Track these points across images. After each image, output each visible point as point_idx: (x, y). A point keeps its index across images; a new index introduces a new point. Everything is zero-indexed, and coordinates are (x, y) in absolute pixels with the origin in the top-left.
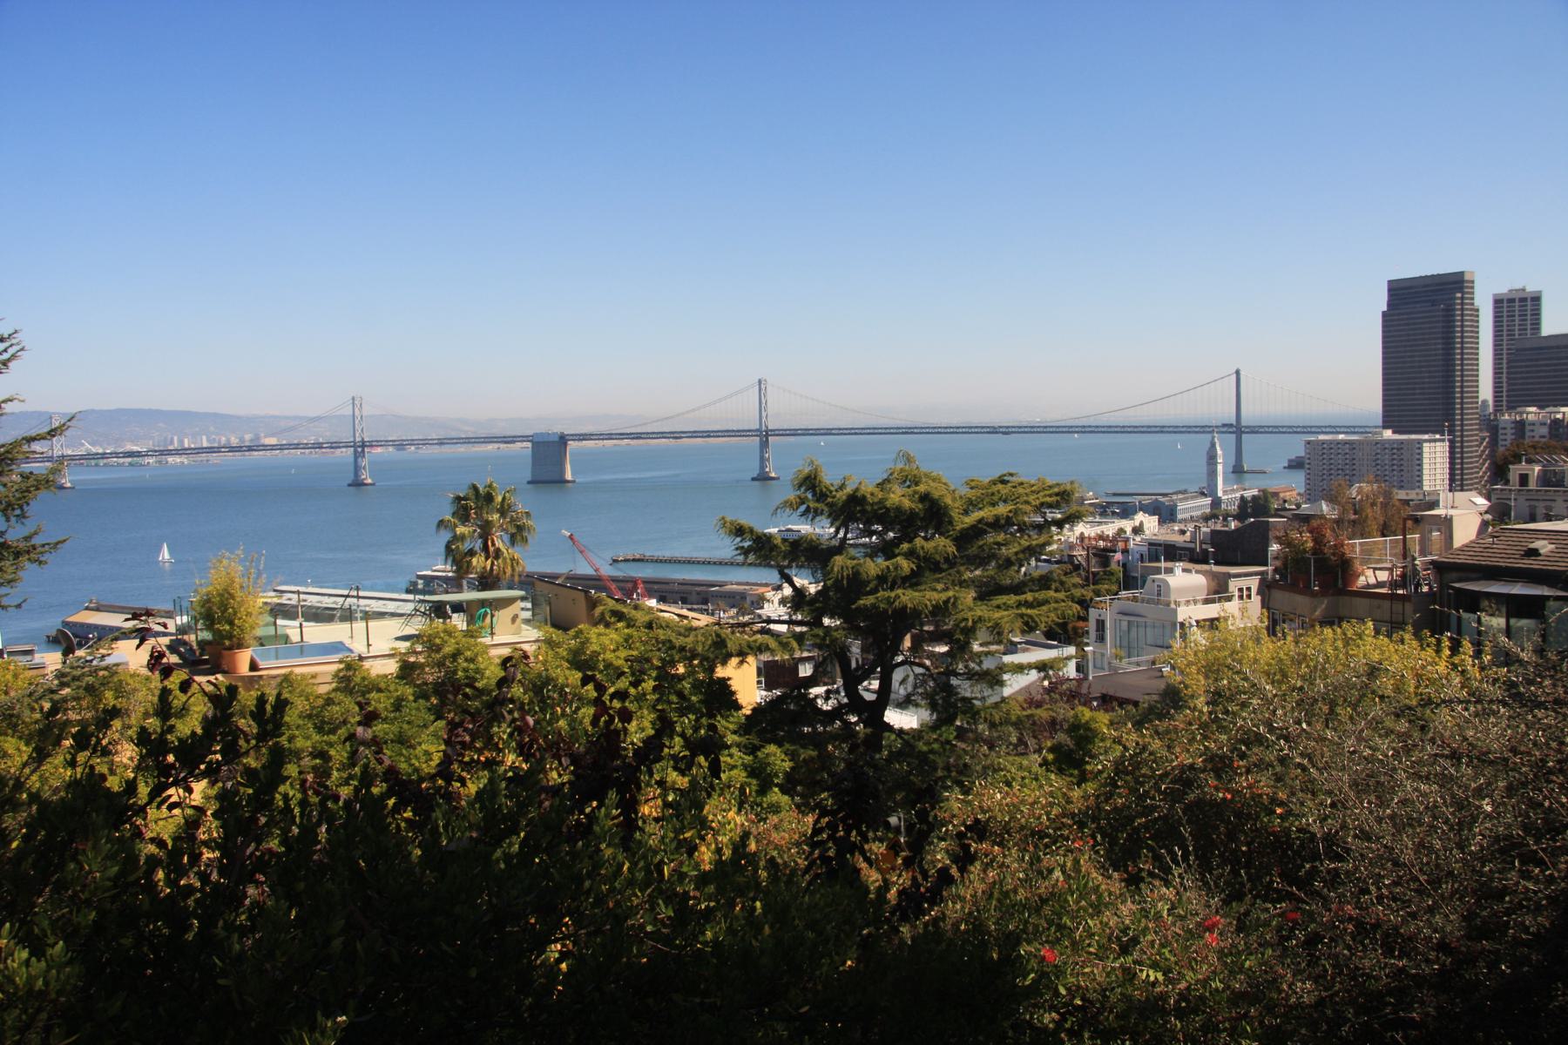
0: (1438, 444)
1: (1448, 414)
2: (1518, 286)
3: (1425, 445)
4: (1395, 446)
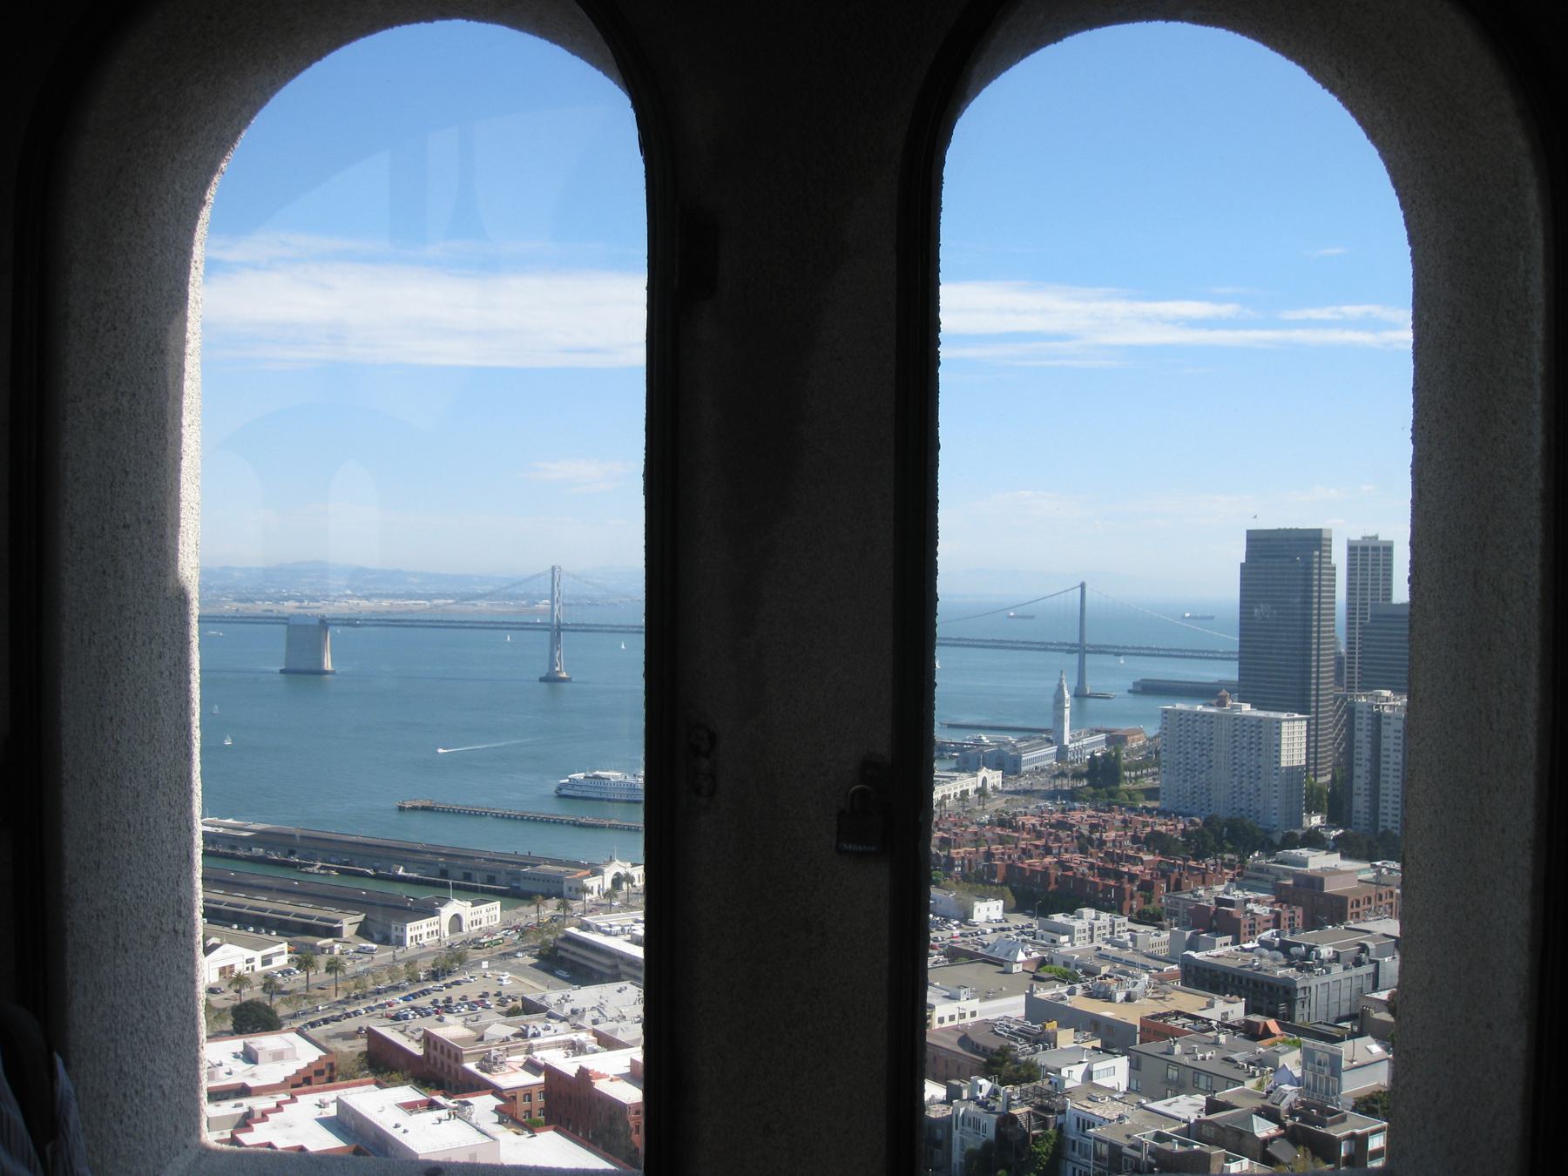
0: (1296, 723)
1: (1305, 693)
2: (1371, 533)
3: (1284, 724)
4: (1254, 723)
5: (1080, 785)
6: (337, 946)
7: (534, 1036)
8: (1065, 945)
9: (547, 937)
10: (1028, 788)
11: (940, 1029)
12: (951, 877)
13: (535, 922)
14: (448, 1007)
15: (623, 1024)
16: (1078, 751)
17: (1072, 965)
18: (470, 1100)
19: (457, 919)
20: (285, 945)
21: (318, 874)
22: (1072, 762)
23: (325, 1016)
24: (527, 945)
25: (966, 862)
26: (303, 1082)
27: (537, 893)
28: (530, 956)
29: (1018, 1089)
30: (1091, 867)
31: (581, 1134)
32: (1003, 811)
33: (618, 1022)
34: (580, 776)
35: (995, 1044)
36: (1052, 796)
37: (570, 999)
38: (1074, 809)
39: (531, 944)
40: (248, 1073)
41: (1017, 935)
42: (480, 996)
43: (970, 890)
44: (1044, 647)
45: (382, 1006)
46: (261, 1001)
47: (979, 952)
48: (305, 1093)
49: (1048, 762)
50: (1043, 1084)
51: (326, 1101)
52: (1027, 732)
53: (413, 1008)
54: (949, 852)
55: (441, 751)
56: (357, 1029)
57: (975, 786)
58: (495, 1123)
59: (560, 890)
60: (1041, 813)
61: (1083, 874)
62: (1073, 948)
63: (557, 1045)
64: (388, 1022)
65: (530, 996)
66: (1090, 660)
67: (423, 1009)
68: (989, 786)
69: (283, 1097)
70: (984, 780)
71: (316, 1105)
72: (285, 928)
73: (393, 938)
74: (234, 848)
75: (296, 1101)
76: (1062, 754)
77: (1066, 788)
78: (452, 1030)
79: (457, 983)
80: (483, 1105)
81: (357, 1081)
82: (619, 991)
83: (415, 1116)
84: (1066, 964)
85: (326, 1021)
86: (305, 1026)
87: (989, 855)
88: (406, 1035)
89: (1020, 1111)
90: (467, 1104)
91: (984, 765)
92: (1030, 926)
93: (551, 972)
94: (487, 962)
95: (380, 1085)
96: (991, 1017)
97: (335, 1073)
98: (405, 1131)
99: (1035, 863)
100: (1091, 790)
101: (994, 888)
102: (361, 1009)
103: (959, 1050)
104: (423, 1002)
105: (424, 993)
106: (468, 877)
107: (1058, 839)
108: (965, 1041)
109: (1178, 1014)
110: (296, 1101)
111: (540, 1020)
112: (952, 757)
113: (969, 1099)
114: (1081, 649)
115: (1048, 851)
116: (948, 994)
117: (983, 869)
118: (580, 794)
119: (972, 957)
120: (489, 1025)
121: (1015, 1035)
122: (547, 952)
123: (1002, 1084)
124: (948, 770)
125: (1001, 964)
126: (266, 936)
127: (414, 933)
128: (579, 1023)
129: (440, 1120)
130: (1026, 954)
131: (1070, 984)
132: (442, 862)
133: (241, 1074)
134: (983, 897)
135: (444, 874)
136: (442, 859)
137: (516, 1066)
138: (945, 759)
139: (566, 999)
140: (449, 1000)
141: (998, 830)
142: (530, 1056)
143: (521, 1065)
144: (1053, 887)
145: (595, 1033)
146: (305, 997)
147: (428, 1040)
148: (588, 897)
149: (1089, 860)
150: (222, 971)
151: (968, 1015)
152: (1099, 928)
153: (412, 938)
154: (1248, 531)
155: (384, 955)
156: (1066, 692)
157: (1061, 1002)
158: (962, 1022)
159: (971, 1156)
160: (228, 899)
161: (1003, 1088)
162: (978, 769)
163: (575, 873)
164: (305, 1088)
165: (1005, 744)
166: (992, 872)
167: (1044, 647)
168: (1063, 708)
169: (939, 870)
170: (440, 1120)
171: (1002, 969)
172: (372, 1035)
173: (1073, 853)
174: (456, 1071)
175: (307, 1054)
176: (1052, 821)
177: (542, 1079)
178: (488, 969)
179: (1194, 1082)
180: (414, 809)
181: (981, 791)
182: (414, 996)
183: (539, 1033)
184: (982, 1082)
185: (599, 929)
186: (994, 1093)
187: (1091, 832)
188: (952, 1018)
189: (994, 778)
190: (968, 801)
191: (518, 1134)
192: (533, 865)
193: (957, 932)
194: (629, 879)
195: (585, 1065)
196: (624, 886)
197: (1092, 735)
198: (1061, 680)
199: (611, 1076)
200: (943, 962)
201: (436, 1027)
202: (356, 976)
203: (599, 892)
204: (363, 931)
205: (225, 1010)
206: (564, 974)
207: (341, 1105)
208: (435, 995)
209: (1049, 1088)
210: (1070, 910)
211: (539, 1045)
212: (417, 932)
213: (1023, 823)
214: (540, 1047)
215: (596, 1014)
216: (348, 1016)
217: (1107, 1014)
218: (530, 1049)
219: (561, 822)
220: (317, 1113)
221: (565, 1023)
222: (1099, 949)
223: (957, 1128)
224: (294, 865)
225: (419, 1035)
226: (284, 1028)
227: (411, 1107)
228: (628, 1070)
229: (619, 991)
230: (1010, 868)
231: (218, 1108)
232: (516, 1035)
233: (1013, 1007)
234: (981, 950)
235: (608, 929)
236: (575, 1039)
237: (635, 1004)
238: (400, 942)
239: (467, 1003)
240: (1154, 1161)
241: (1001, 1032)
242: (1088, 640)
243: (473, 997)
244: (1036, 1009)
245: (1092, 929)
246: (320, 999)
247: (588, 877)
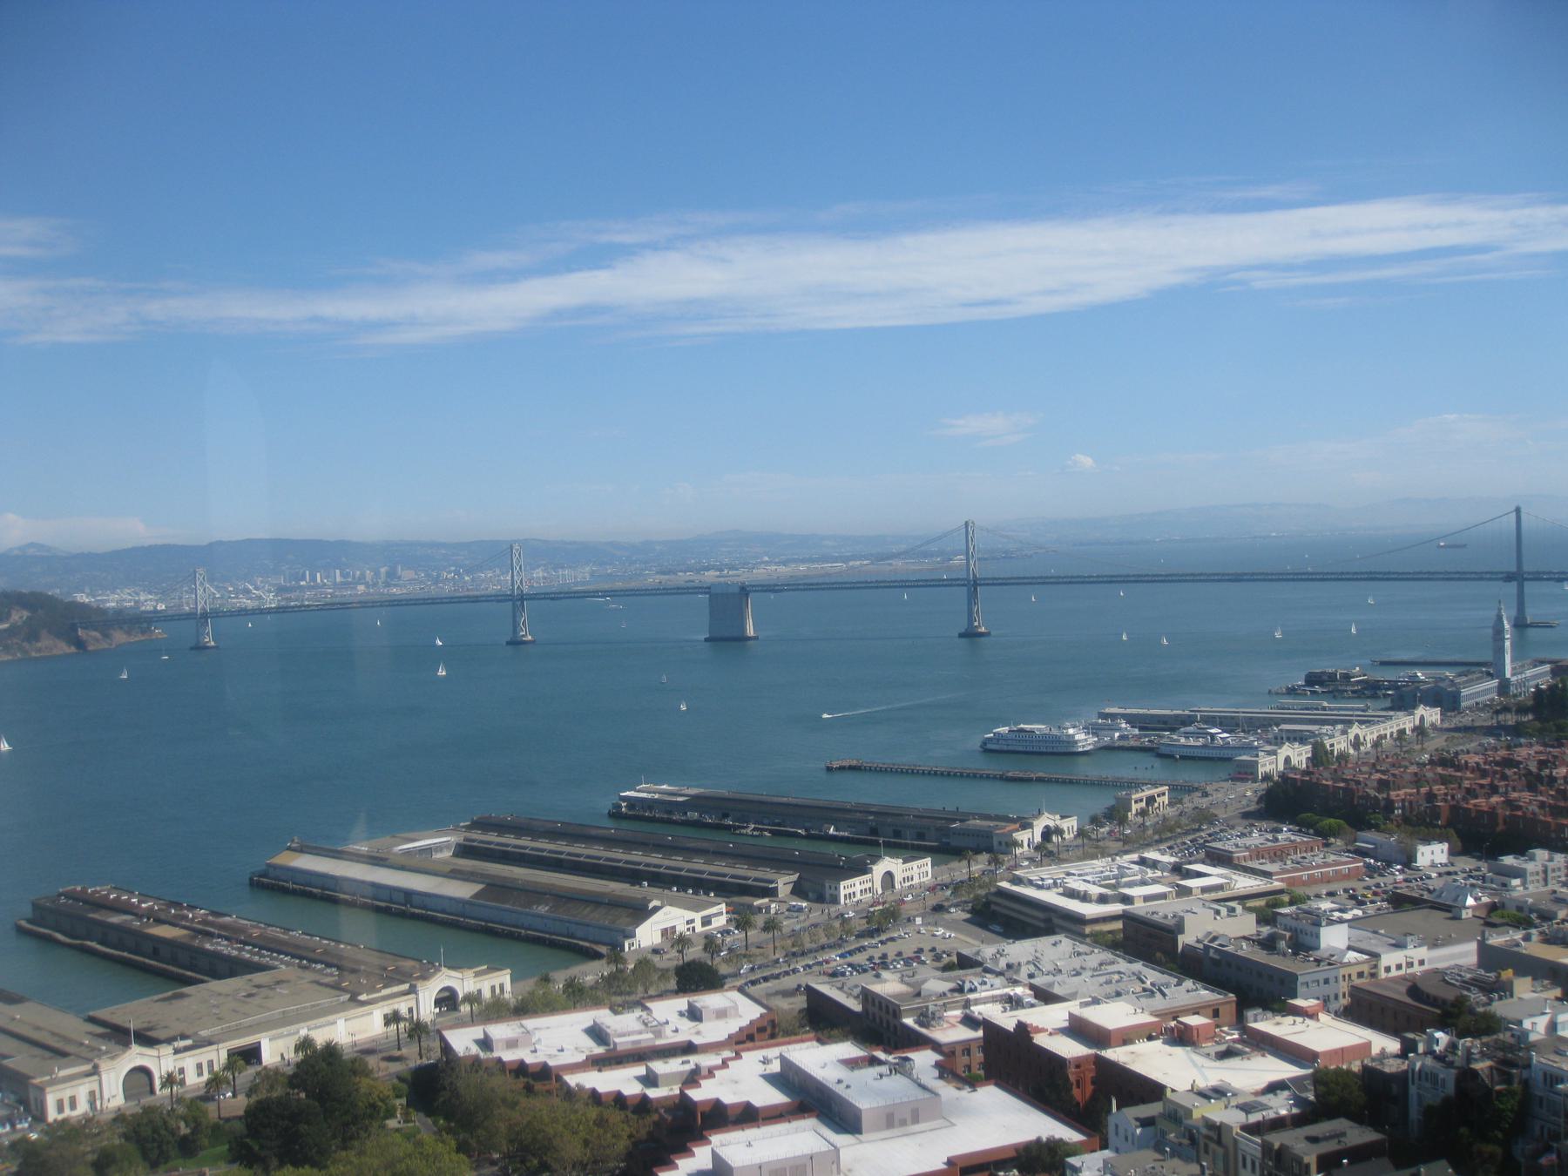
5: (1525, 719)
6: (773, 905)
7: (972, 990)
8: (1518, 888)
9: (979, 892)
10: (1470, 724)
11: (1387, 979)
12: (1391, 820)
13: (967, 877)
14: (884, 963)
15: (1059, 978)
16: (1522, 683)
17: (1526, 909)
18: (910, 1055)
19: (889, 876)
20: (724, 905)
21: (752, 836)
22: (1515, 696)
23: (765, 974)
24: (959, 900)
25: (1407, 804)
26: (747, 1039)
27: (967, 849)
28: (963, 910)
29: (1477, 1042)
30: (1542, 805)
31: (1021, 1088)
32: (1443, 750)
33: (1054, 976)
34: (1004, 730)
35: (1450, 995)
36: (1489, 731)
37: (1005, 953)
38: (1521, 745)
39: (963, 899)
40: (694, 1031)
41: (1464, 879)
42: (915, 952)
43: (1412, 834)
44: (1480, 577)
45: (820, 964)
46: (702, 960)
47: (1425, 897)
48: (749, 1049)
49: (1489, 697)
50: (1504, 1037)
51: (769, 1057)
52: (1466, 667)
53: (850, 965)
54: (1388, 795)
55: (825, 716)
56: (796, 986)
58: (936, 1078)
59: (993, 846)
60: (1484, 750)
61: (1534, 813)
62: (1526, 892)
63: (994, 999)
64: (826, 979)
65: (966, 952)
66: (1529, 587)
67: (859, 966)
68: (1427, 725)
69: (727, 1054)
70: (1422, 718)
71: (760, 1061)
72: (723, 889)
73: (827, 896)
74: (670, 812)
75: (741, 1058)
76: (1504, 687)
77: (1510, 723)
78: (889, 986)
79: (892, 939)
80: (923, 1060)
81: (799, 1037)
82: (1054, 945)
83: (857, 1073)
84: (1520, 909)
85: (766, 979)
86: (746, 984)
87: (1431, 797)
88: (845, 992)
89: (1481, 1066)
90: (907, 1059)
91: (1421, 702)
92: (1478, 869)
93: (983, 925)
94: (920, 919)
95: (821, 1042)
96: (1441, 965)
97: (777, 1030)
98: (848, 1087)
99: (1481, 801)
100: (1538, 724)
101: (1438, 830)
102: (799, 967)
103: (1409, 1000)
104: (860, 958)
105: (861, 949)
106: (897, 834)
107: (1504, 777)
108: (1415, 990)
110: (741, 1058)
111: (976, 975)
112: (1386, 696)
113: (1425, 1053)
114: (1516, 577)
115: (1494, 790)
116: (1394, 942)
117: (1426, 812)
118: (1005, 748)
119: (1416, 903)
120: (924, 981)
121: (1467, 984)
122: (979, 907)
123: (1461, 1035)
124: (1383, 710)
125: (1450, 909)
126: (704, 898)
127: (847, 891)
128: (1015, 977)
129: (881, 1076)
130: (1476, 899)
131: (1525, 929)
132: (871, 821)
133: (686, 1031)
134: (1427, 840)
135: (874, 832)
136: (871, 818)
137: (953, 1021)
138: (1379, 697)
139: (1000, 953)
140: (884, 956)
141: (1439, 770)
142: (968, 1011)
143: (959, 1020)
144: (1500, 827)
145: (1032, 987)
146: (745, 956)
147: (867, 997)
148: (1018, 851)
149: (1541, 798)
150: (665, 932)
152: (1553, 871)
153: (845, 896)
155: (816, 914)
156: (1505, 622)
157: (1516, 949)
158: (1410, 971)
159: (1429, 1112)
160: (667, 863)
161: (1463, 1041)
162: (1415, 707)
163: (1004, 828)
164: (749, 1044)
165: (1442, 680)
166: (1435, 812)
167: (1480, 577)
168: (1503, 639)
169: (1378, 813)
170: (881, 1076)
171: (1449, 915)
172: (811, 993)
173: (1520, 791)
174: (895, 1027)
175: (749, 1012)
176: (1497, 758)
177: (980, 1033)
178: (922, 925)
180: (842, 768)
181: (1420, 730)
182: (850, 953)
183: (976, 987)
184: (1439, 1035)
185: (1031, 883)
186: (1452, 1047)
187: (1540, 769)
188: (1399, 967)
189: (1432, 715)
190: (1405, 740)
191: (959, 1089)
192: (961, 821)
193: (1400, 877)
194: (1059, 831)
195: (1023, 1019)
196: (1054, 838)
197: (1535, 666)
198: (1500, 609)
199: (1050, 1030)
200: (1386, 908)
201: (873, 983)
202: (794, 933)
203: (1029, 846)
204: (798, 891)
205: (667, 970)
206: (998, 928)
207: (785, 1062)
208: (871, 952)
209: (1512, 1041)
210: (1521, 850)
211: (976, 1000)
212: (851, 890)
213: (1466, 762)
214: (977, 1002)
215: (1032, 968)
216: (787, 973)
218: (967, 1004)
219: (988, 777)
220: (761, 1069)
221: (1002, 977)
222: (1555, 892)
223: (1413, 1083)
224: (728, 827)
225: (857, 991)
226: (726, 987)
227: (852, 1064)
228: (1066, 1024)
229: (1054, 945)
230: (1455, 809)
231: (667, 1065)
232: (952, 990)
233: (1462, 955)
234: (1426, 896)
235: (1040, 883)
236: (1012, 993)
237: (1070, 957)
238: (835, 900)
239: (903, 959)
241: (1453, 981)
242: (1527, 567)
243: (909, 953)
244: (1490, 958)
245: (1545, 872)
246: (759, 958)
247: (1017, 830)
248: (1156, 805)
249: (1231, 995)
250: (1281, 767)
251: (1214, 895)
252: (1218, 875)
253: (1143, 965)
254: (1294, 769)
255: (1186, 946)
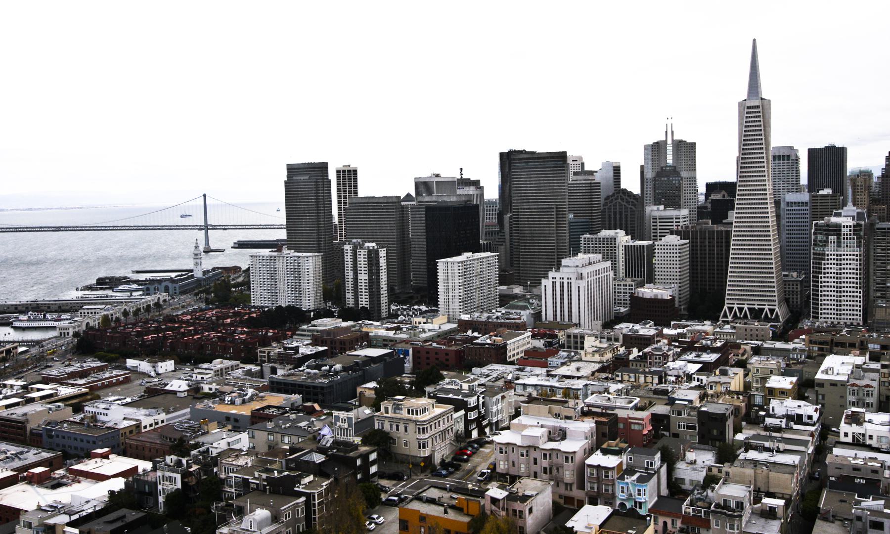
57: (154, 302)
109: (269, 407)
151: (160, 422)
154: (287, 165)
158: (157, 426)
179: (282, 440)
181: (157, 305)
188: (151, 425)
217: (234, 412)
240: (266, 483)
248: (12, 354)
249: (59, 453)
250: (84, 328)
251: (47, 400)
252: (50, 389)
253: (6, 444)
254: (92, 328)
255: (32, 430)
